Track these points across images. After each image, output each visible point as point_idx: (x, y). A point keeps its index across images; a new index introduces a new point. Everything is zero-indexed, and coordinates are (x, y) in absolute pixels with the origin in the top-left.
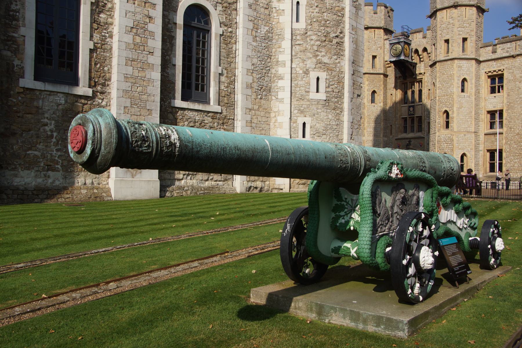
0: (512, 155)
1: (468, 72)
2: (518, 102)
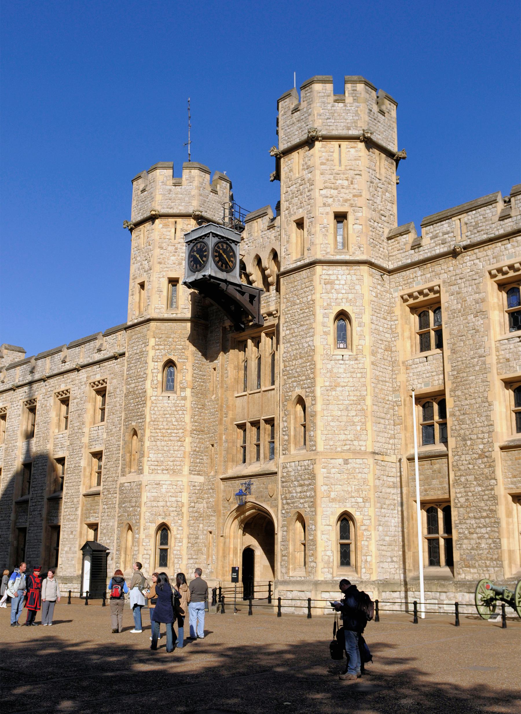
0: (471, 515)
1: (350, 296)
2: (477, 368)
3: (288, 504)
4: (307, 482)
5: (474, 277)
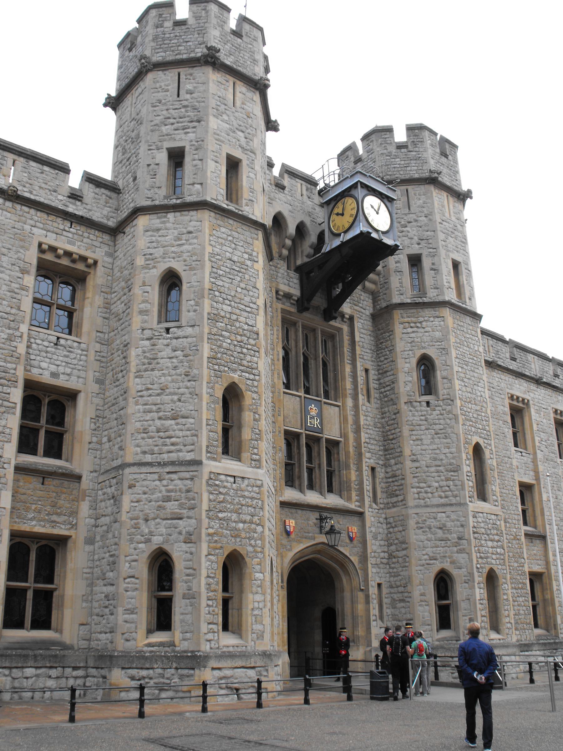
3: (481, 558)
4: (497, 538)
5: (501, 392)
